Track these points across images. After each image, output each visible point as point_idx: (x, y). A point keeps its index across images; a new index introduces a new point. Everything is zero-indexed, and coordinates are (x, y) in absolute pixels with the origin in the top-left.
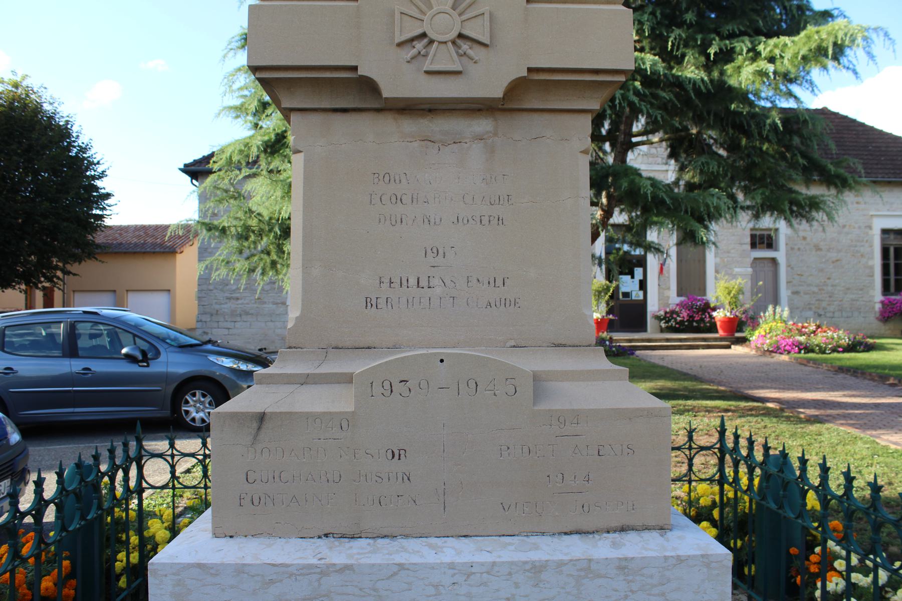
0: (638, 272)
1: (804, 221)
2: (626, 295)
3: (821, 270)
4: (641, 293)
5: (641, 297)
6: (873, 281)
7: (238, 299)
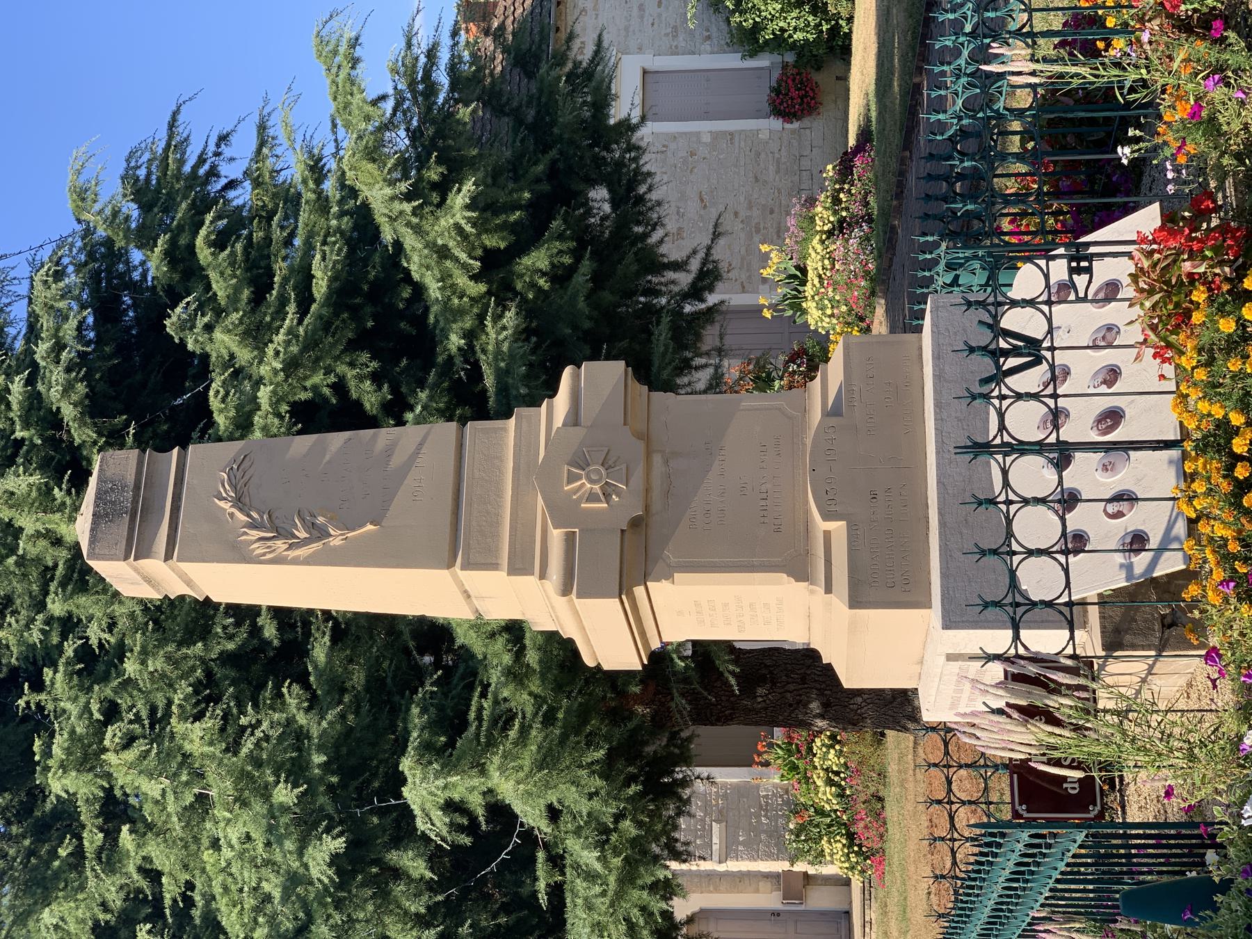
6: (740, 132)
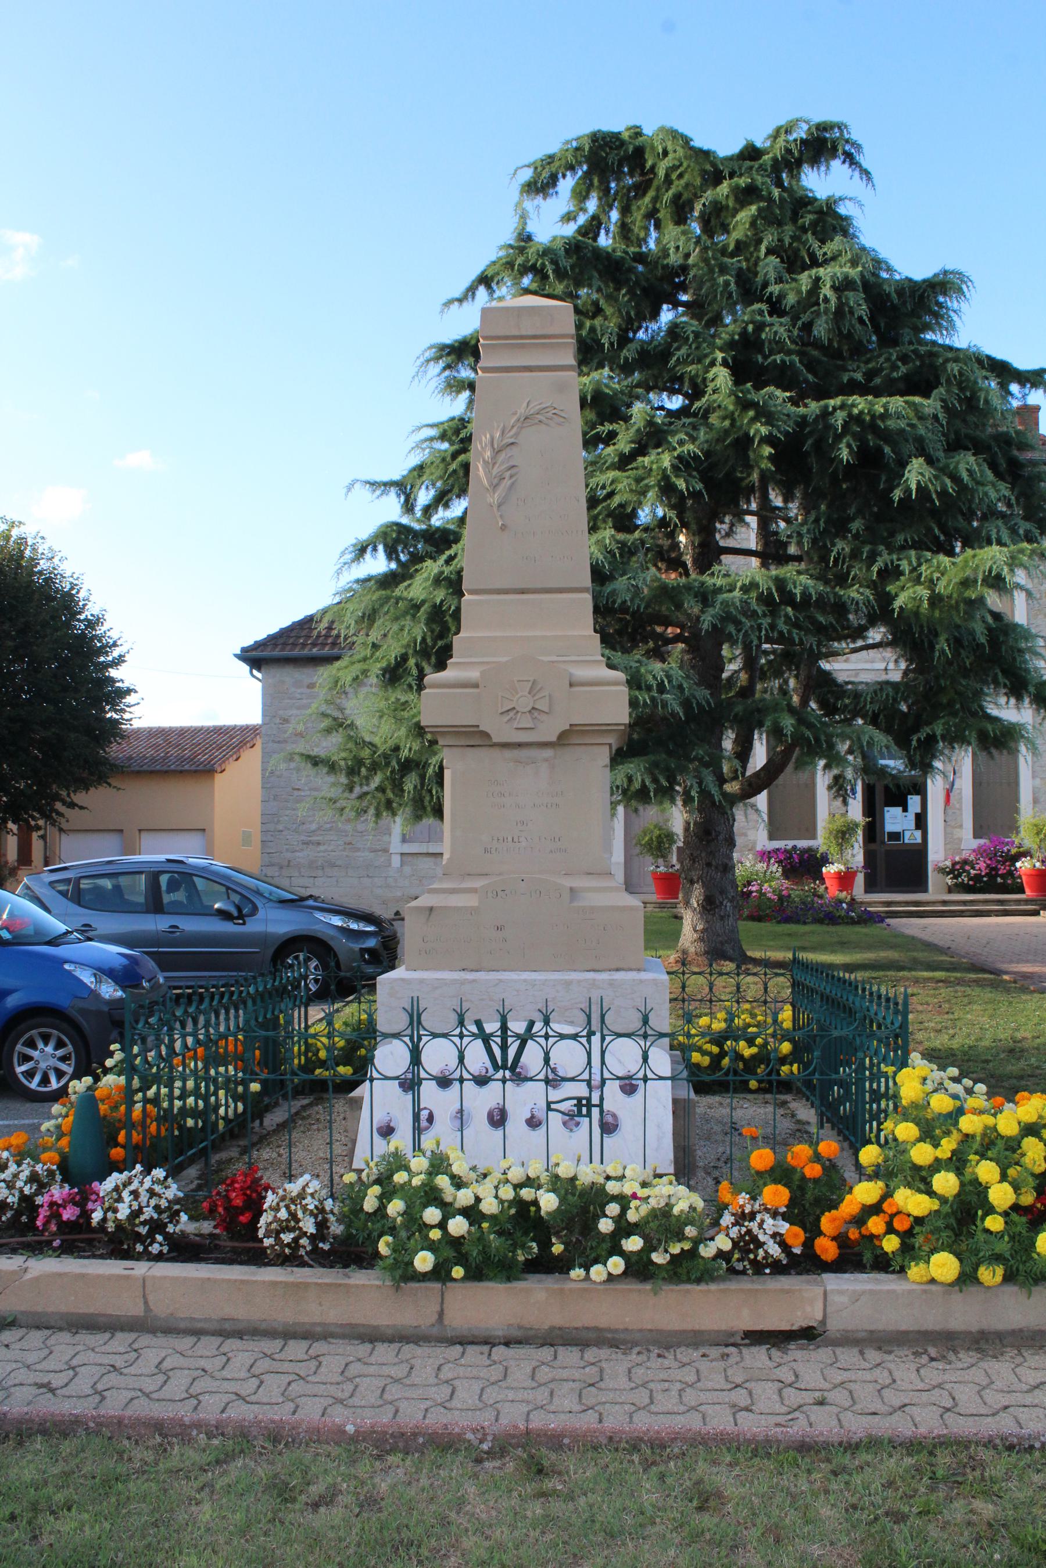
0: (914, 802)
2: (896, 836)
4: (918, 834)
5: (919, 840)
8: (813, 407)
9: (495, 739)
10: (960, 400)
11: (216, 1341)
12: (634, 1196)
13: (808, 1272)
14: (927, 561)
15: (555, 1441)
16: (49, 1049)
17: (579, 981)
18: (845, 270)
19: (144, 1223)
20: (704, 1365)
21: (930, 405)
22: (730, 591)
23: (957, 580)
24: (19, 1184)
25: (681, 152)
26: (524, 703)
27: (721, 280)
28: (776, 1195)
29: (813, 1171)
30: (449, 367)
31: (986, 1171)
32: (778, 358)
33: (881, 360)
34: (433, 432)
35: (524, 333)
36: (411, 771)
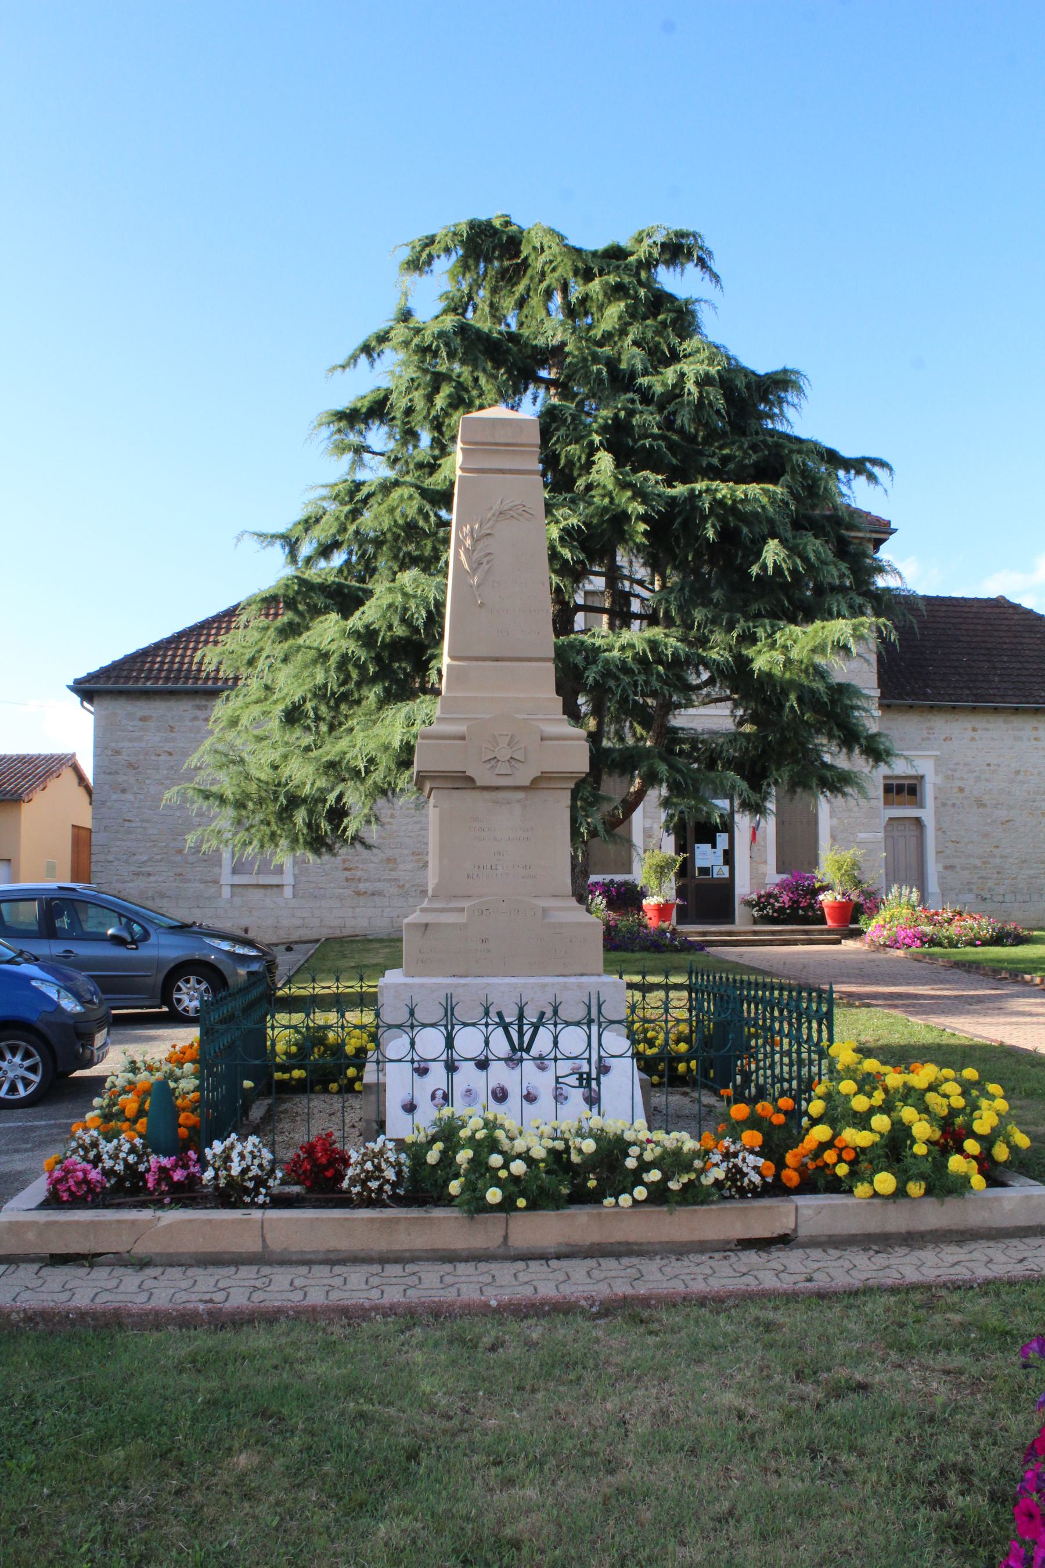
0: (722, 839)
1: (840, 796)
2: (705, 871)
3: (986, 835)
4: (726, 869)
5: (727, 875)
7: (149, 875)
8: (680, 490)
9: (478, 784)
10: (803, 487)
11: (328, 1268)
12: (649, 1141)
13: (776, 1196)
14: (780, 629)
15: (645, 1301)
16: (17, 1060)
17: (553, 984)
18: (705, 367)
19: (250, 1179)
20: (712, 1263)
21: (778, 490)
22: (610, 650)
23: (809, 647)
24: (122, 1155)
25: (556, 249)
26: (504, 754)
27: (595, 368)
28: (752, 1138)
29: (779, 1119)
30: (339, 431)
31: (908, 1114)
32: (647, 442)
33: (735, 448)
34: (324, 492)
35: (497, 441)
36: (297, 806)
